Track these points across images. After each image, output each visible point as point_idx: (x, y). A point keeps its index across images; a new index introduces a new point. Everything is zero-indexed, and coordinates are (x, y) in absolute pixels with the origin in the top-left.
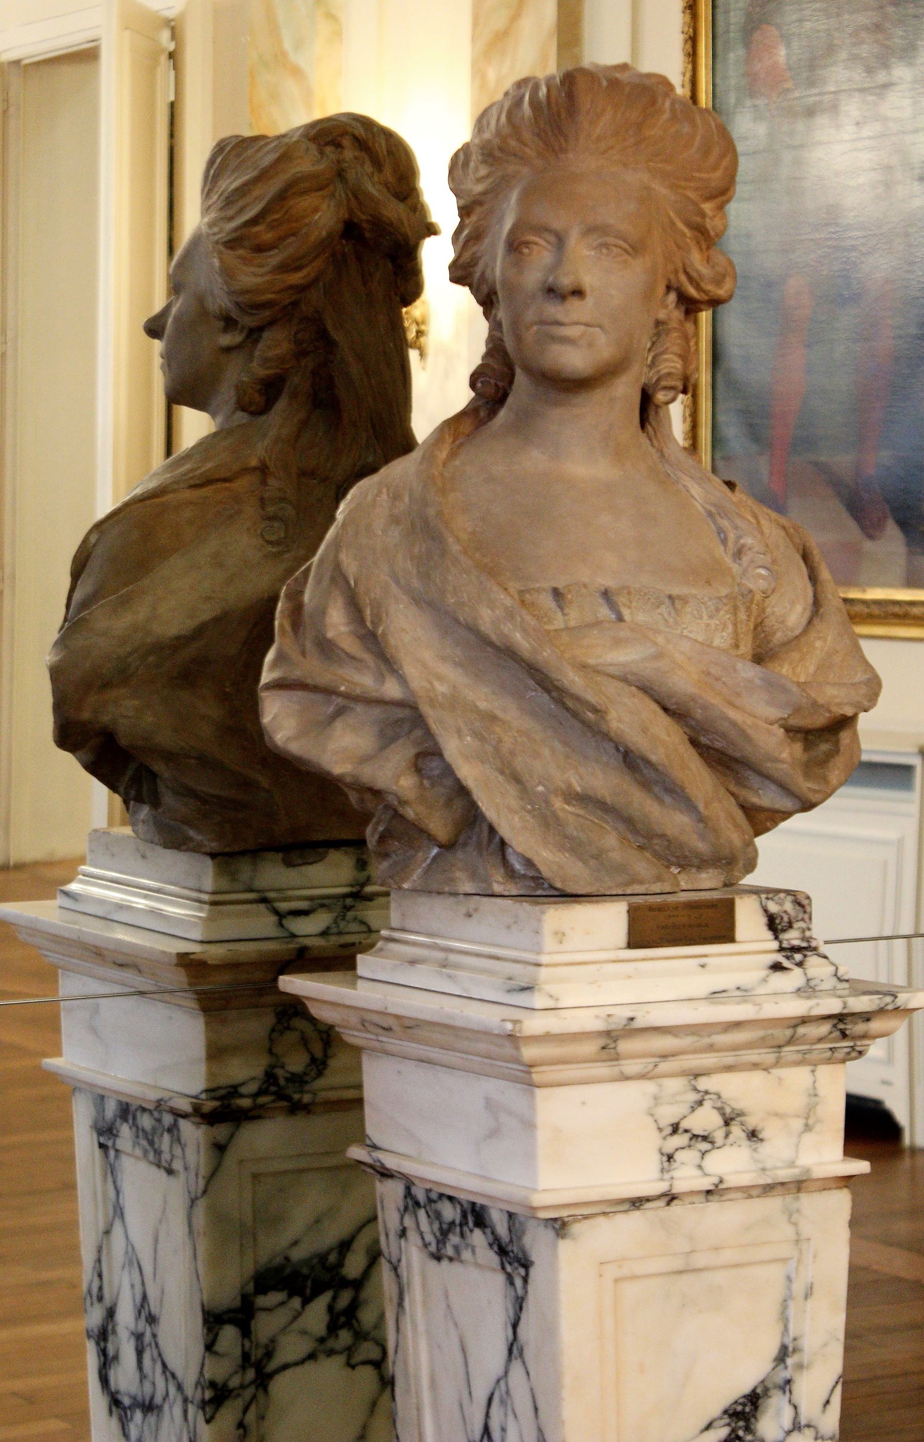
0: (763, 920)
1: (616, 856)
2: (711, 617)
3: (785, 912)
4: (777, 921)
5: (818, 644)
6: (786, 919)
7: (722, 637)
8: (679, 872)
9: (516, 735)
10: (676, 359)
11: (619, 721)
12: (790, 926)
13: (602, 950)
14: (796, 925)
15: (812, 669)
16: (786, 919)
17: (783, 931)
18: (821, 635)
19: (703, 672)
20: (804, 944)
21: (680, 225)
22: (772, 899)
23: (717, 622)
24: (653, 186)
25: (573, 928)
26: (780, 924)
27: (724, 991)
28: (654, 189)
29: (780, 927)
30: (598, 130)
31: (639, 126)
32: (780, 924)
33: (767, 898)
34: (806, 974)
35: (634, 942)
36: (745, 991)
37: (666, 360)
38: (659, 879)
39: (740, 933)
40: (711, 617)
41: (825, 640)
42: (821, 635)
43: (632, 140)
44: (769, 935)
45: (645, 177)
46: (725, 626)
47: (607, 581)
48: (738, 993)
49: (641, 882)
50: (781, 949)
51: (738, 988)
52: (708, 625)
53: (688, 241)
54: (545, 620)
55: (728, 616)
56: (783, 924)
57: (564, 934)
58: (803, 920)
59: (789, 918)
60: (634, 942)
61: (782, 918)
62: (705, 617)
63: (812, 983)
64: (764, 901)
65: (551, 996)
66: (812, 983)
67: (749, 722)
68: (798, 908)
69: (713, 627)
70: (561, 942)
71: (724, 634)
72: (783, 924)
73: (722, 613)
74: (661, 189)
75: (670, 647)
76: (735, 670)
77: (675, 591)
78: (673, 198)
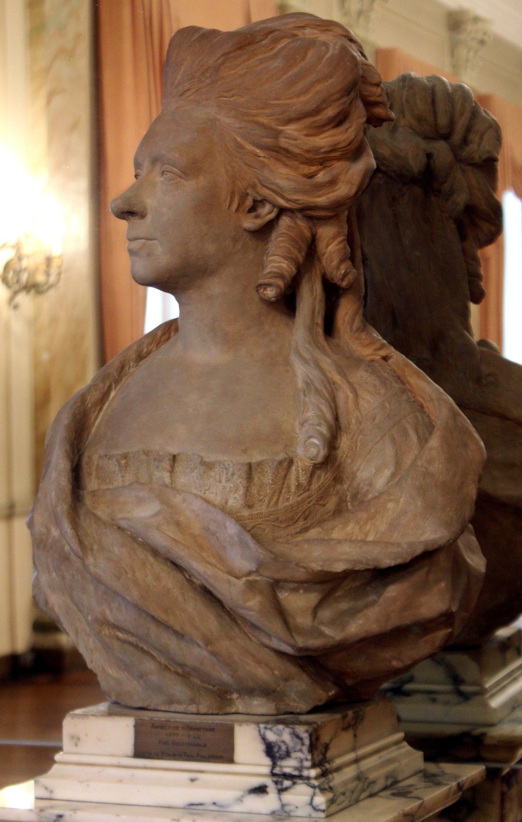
0: (261, 747)
1: (154, 678)
2: (228, 481)
3: (283, 742)
4: (276, 750)
5: (390, 505)
6: (284, 748)
7: (235, 498)
8: (237, 698)
9: (74, 573)
10: (282, 260)
11: (95, 567)
12: (288, 754)
13: (112, 755)
14: (294, 755)
15: (383, 527)
16: (284, 748)
17: (282, 758)
18: (392, 497)
19: (204, 528)
20: (296, 773)
21: (250, 147)
22: (271, 729)
23: (232, 485)
24: (218, 117)
25: (87, 735)
26: (278, 752)
27: (201, 804)
28: (219, 120)
29: (277, 755)
30: (179, 77)
31: (217, 69)
32: (278, 752)
33: (266, 728)
34: (280, 800)
35: (140, 752)
36: (221, 806)
37: (272, 261)
38: (192, 701)
39: (239, 754)
40: (228, 481)
41: (397, 502)
42: (392, 497)
43: (208, 81)
44: (268, 761)
45: (211, 111)
46: (237, 490)
47: (174, 450)
48: (214, 808)
49: (179, 702)
50: (273, 774)
51: (214, 804)
52: (224, 488)
53: (266, 160)
54: (107, 480)
55: (240, 480)
56: (281, 753)
57: (79, 739)
58: (301, 751)
59: (287, 748)
60: (140, 752)
61: (280, 747)
62: (223, 480)
63: (287, 808)
64: (262, 731)
65: (46, 788)
66: (287, 808)
67: (209, 573)
68: (296, 740)
69: (228, 489)
70: (76, 745)
71: (236, 495)
72: (281, 753)
73: (235, 477)
74: (226, 120)
75: (184, 505)
76: (226, 527)
77: (210, 458)
78: (237, 125)
